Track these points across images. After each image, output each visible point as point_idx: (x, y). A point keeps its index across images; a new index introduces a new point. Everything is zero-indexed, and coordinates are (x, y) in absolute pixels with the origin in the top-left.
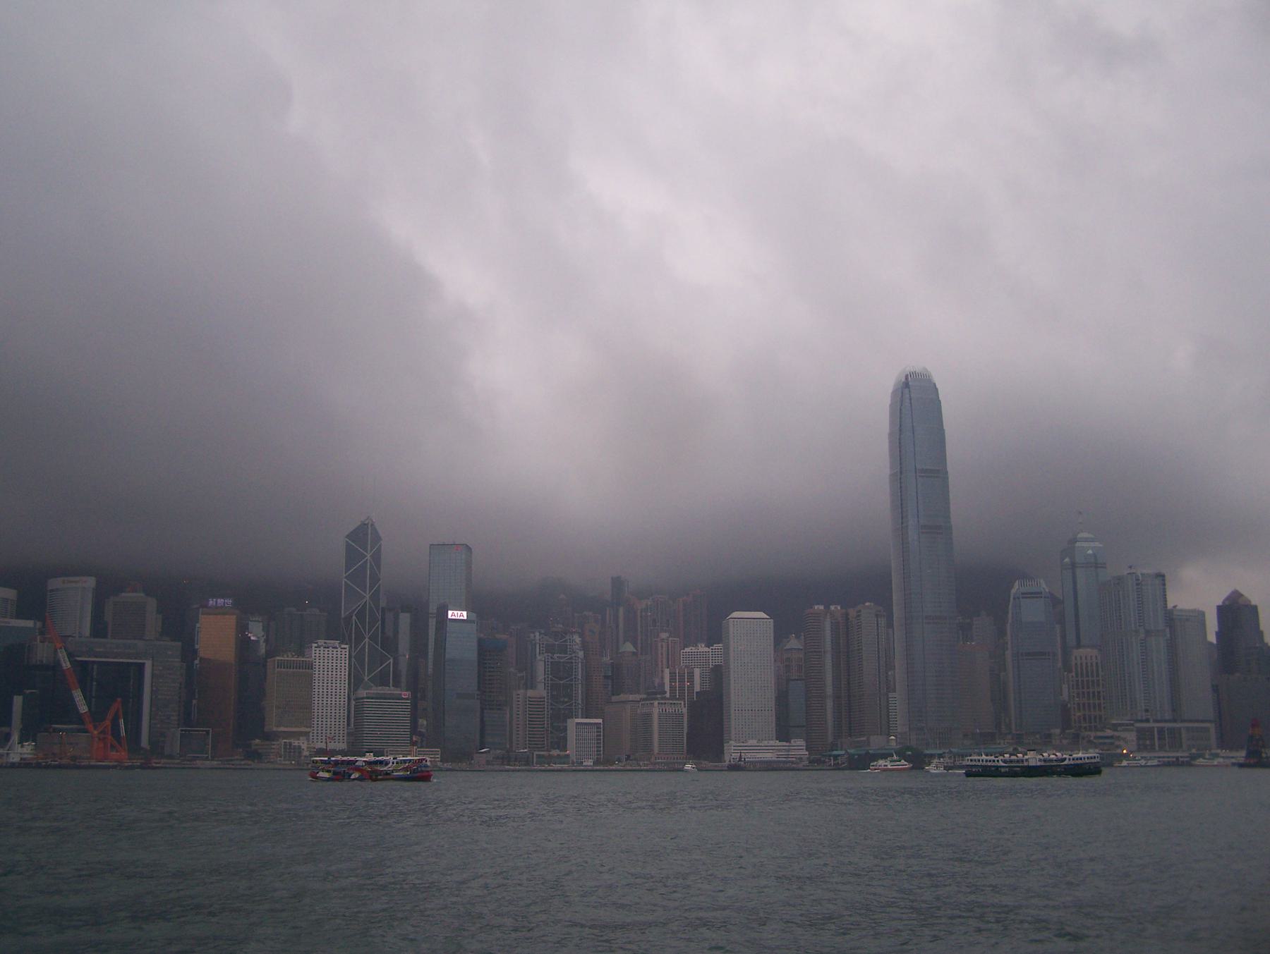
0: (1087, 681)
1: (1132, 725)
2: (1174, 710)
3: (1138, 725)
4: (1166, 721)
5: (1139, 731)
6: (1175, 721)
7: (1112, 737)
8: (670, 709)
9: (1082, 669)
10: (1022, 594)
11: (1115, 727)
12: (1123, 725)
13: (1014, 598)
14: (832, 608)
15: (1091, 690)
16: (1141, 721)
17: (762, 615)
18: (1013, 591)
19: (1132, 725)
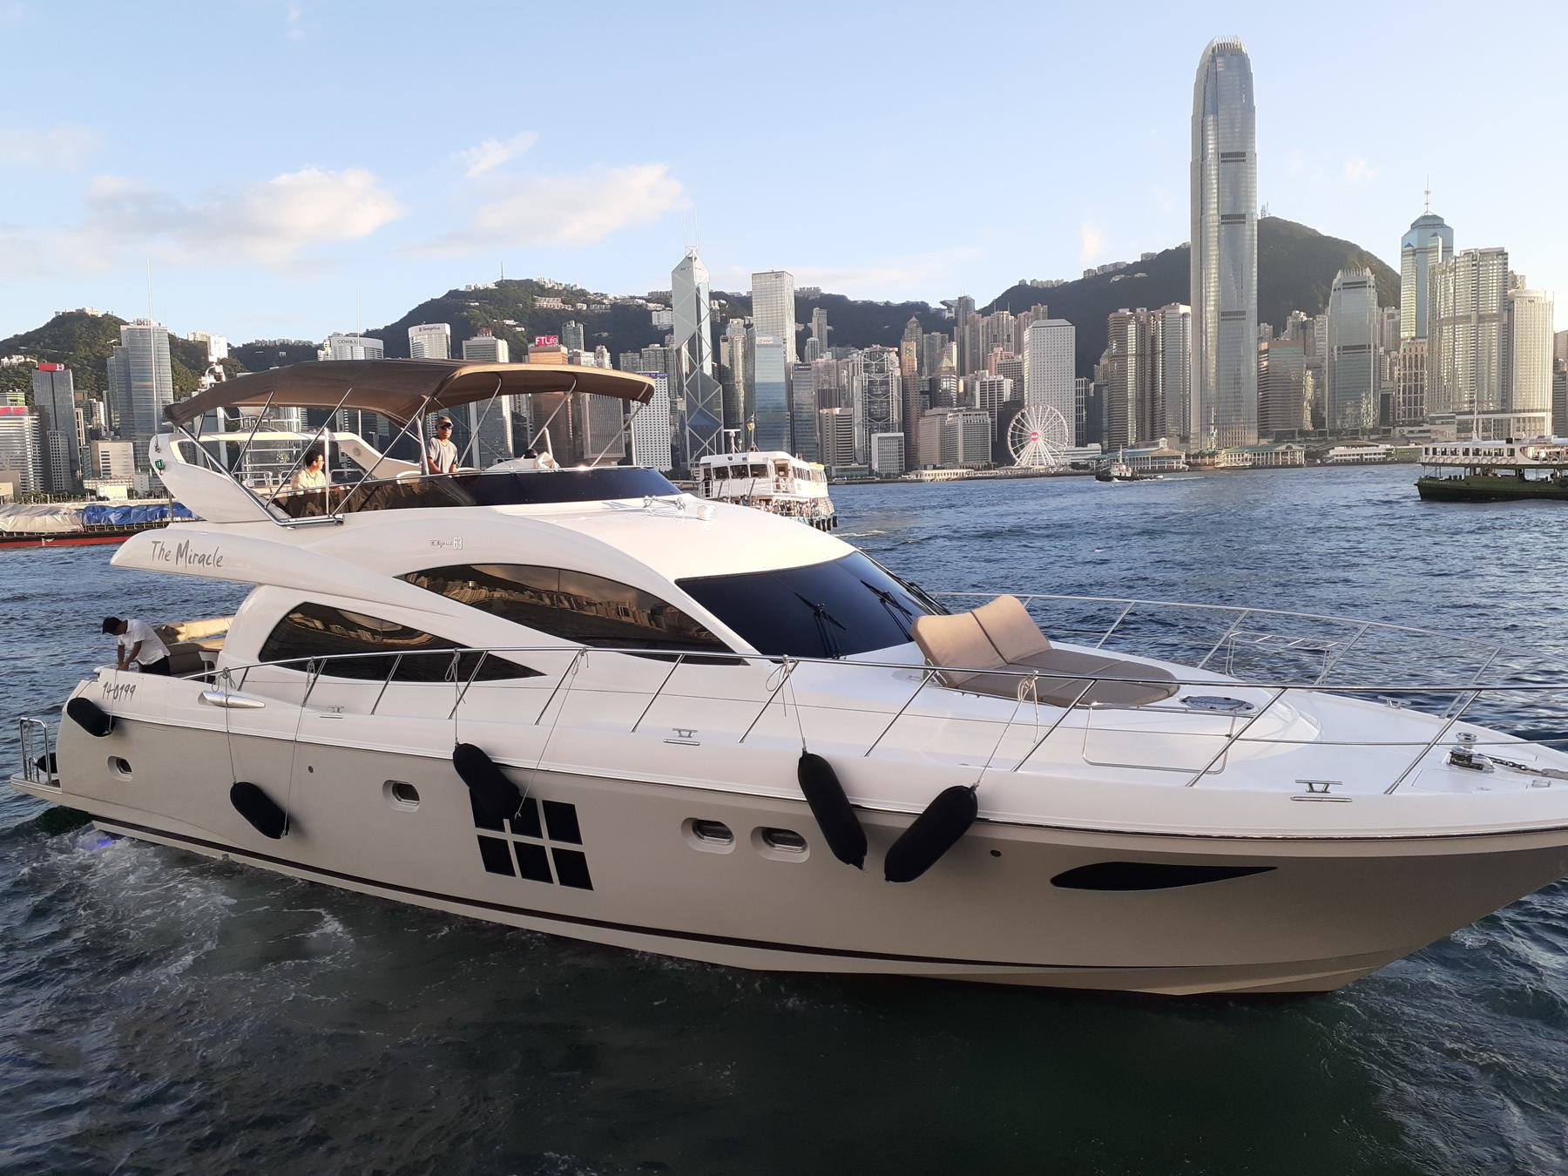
0: (1415, 373)
1: (1454, 417)
2: (1503, 401)
3: (1458, 417)
4: (1493, 412)
5: (1460, 423)
6: (1503, 411)
7: (1429, 431)
8: (974, 419)
9: (1416, 361)
10: (1344, 284)
11: (1433, 421)
12: (1443, 418)
13: (1335, 290)
14: (1138, 310)
15: (1408, 384)
16: (1465, 413)
17: (1063, 322)
18: (1335, 281)
19: (1454, 417)
